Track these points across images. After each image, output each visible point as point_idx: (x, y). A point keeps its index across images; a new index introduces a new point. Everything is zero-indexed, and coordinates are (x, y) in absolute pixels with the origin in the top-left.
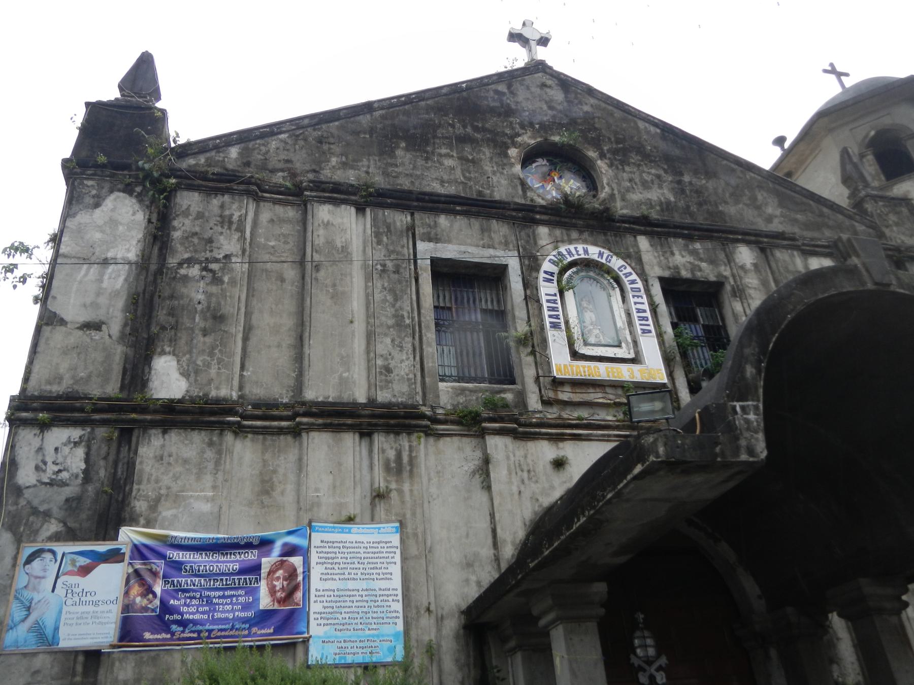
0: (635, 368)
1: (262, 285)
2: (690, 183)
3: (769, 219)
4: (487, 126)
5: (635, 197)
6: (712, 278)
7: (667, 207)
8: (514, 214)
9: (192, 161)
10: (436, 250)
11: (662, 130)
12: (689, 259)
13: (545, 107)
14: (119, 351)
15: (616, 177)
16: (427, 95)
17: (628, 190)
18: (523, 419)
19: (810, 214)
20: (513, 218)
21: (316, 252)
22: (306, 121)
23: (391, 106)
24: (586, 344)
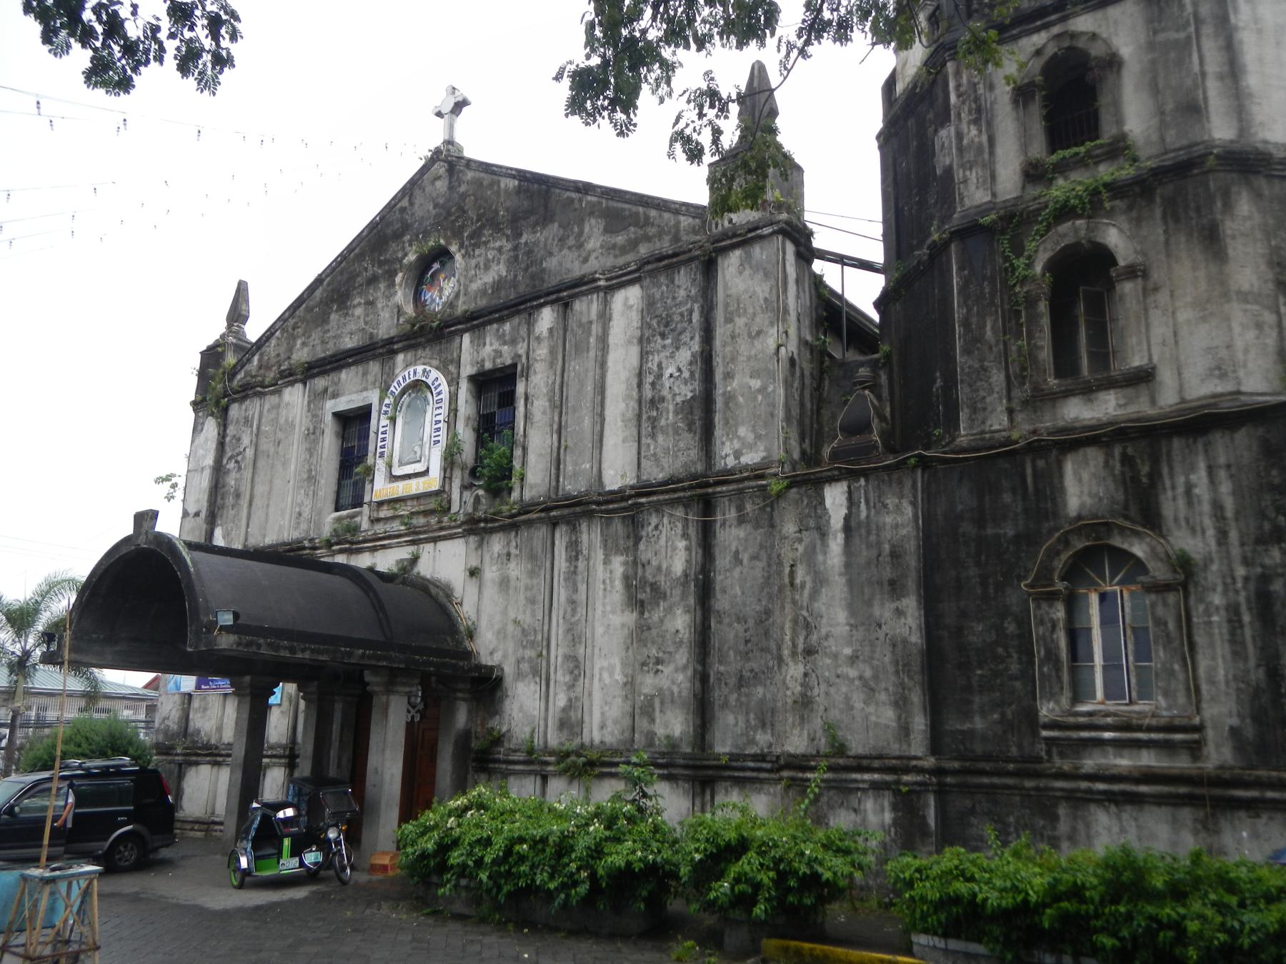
0: (421, 480)
1: (261, 463)
2: (526, 243)
3: (586, 260)
4: (388, 256)
5: (474, 286)
6: (509, 362)
7: (498, 285)
8: (381, 351)
9: (238, 377)
10: (335, 405)
11: (520, 180)
12: (496, 346)
13: (431, 207)
14: (204, 526)
15: (466, 270)
16: (354, 245)
17: (471, 281)
18: (355, 539)
19: (632, 229)
20: (381, 355)
21: (280, 430)
22: (287, 314)
23: (334, 269)
24: (401, 464)
